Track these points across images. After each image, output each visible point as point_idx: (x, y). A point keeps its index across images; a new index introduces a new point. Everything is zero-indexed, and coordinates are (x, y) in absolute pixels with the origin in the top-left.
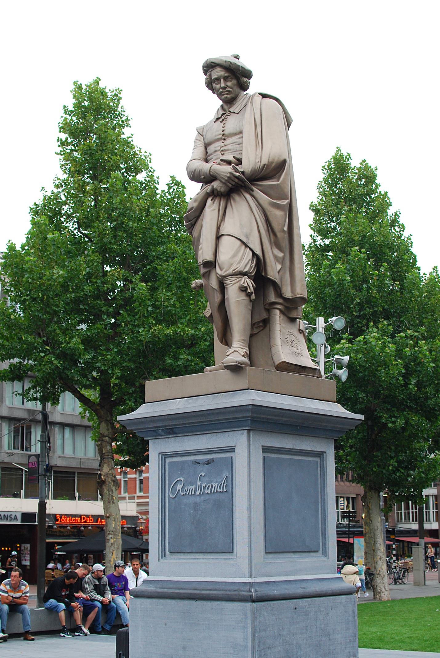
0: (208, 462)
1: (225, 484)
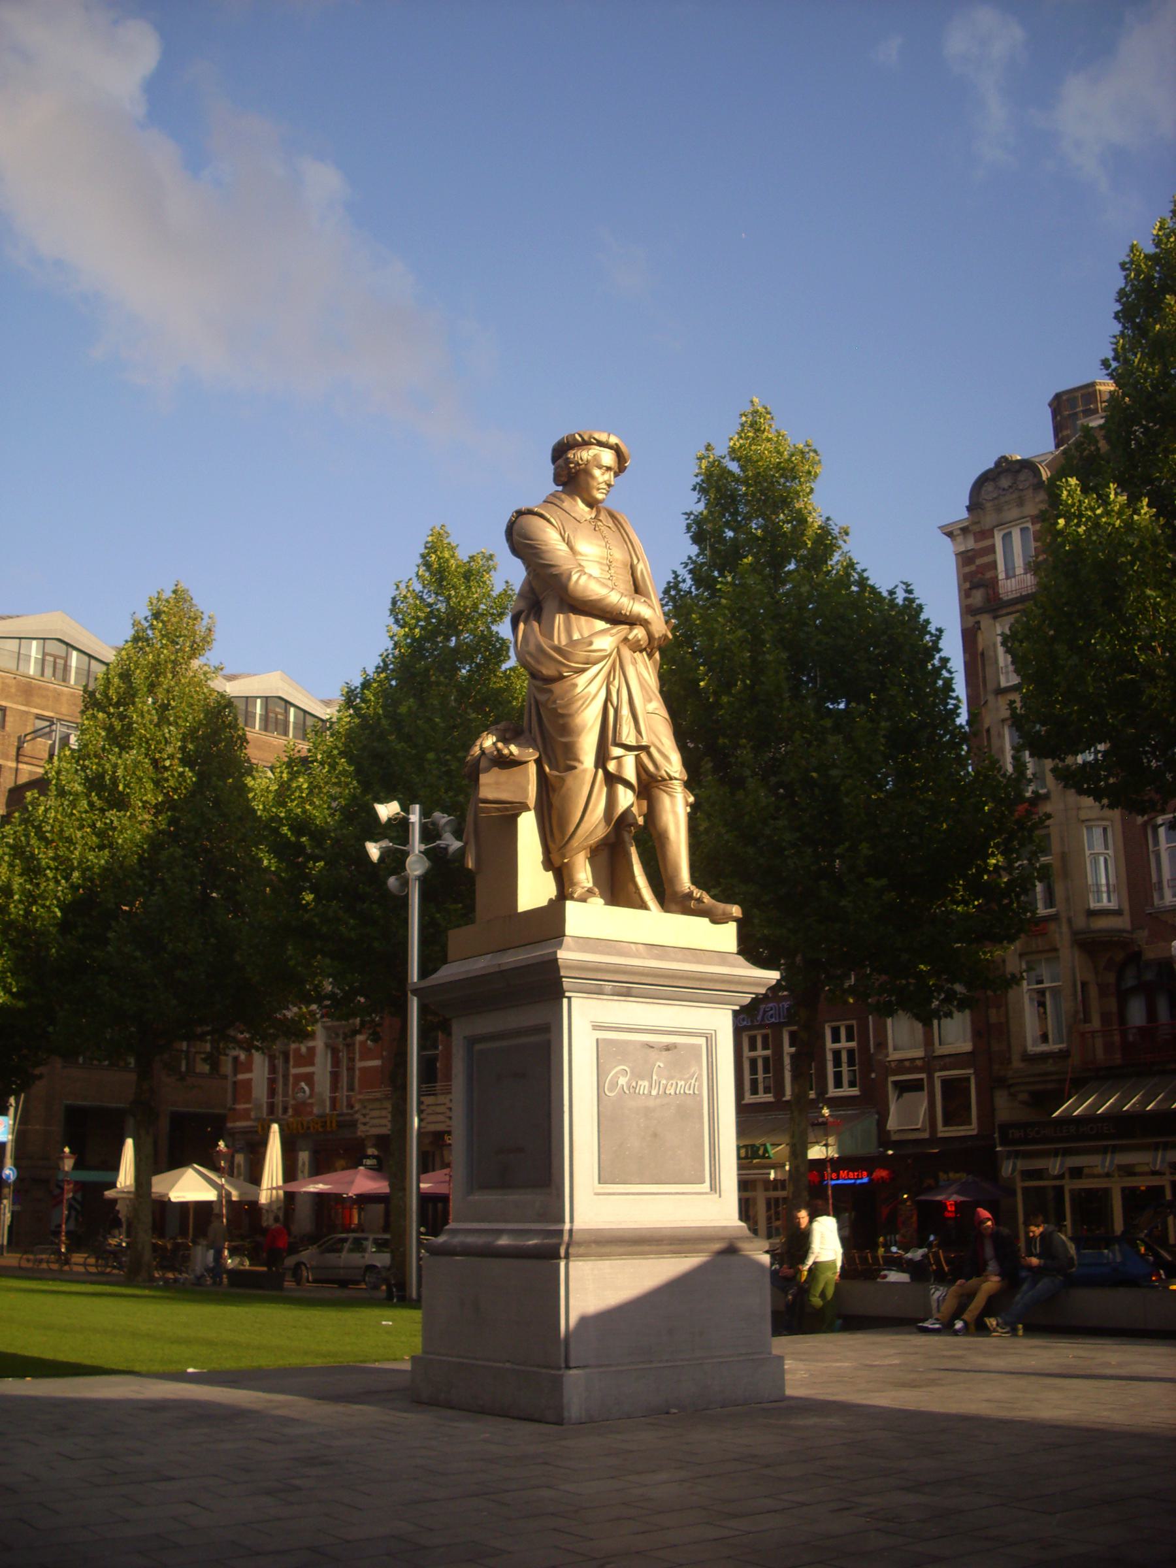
0: (668, 1048)
1: (697, 1084)
